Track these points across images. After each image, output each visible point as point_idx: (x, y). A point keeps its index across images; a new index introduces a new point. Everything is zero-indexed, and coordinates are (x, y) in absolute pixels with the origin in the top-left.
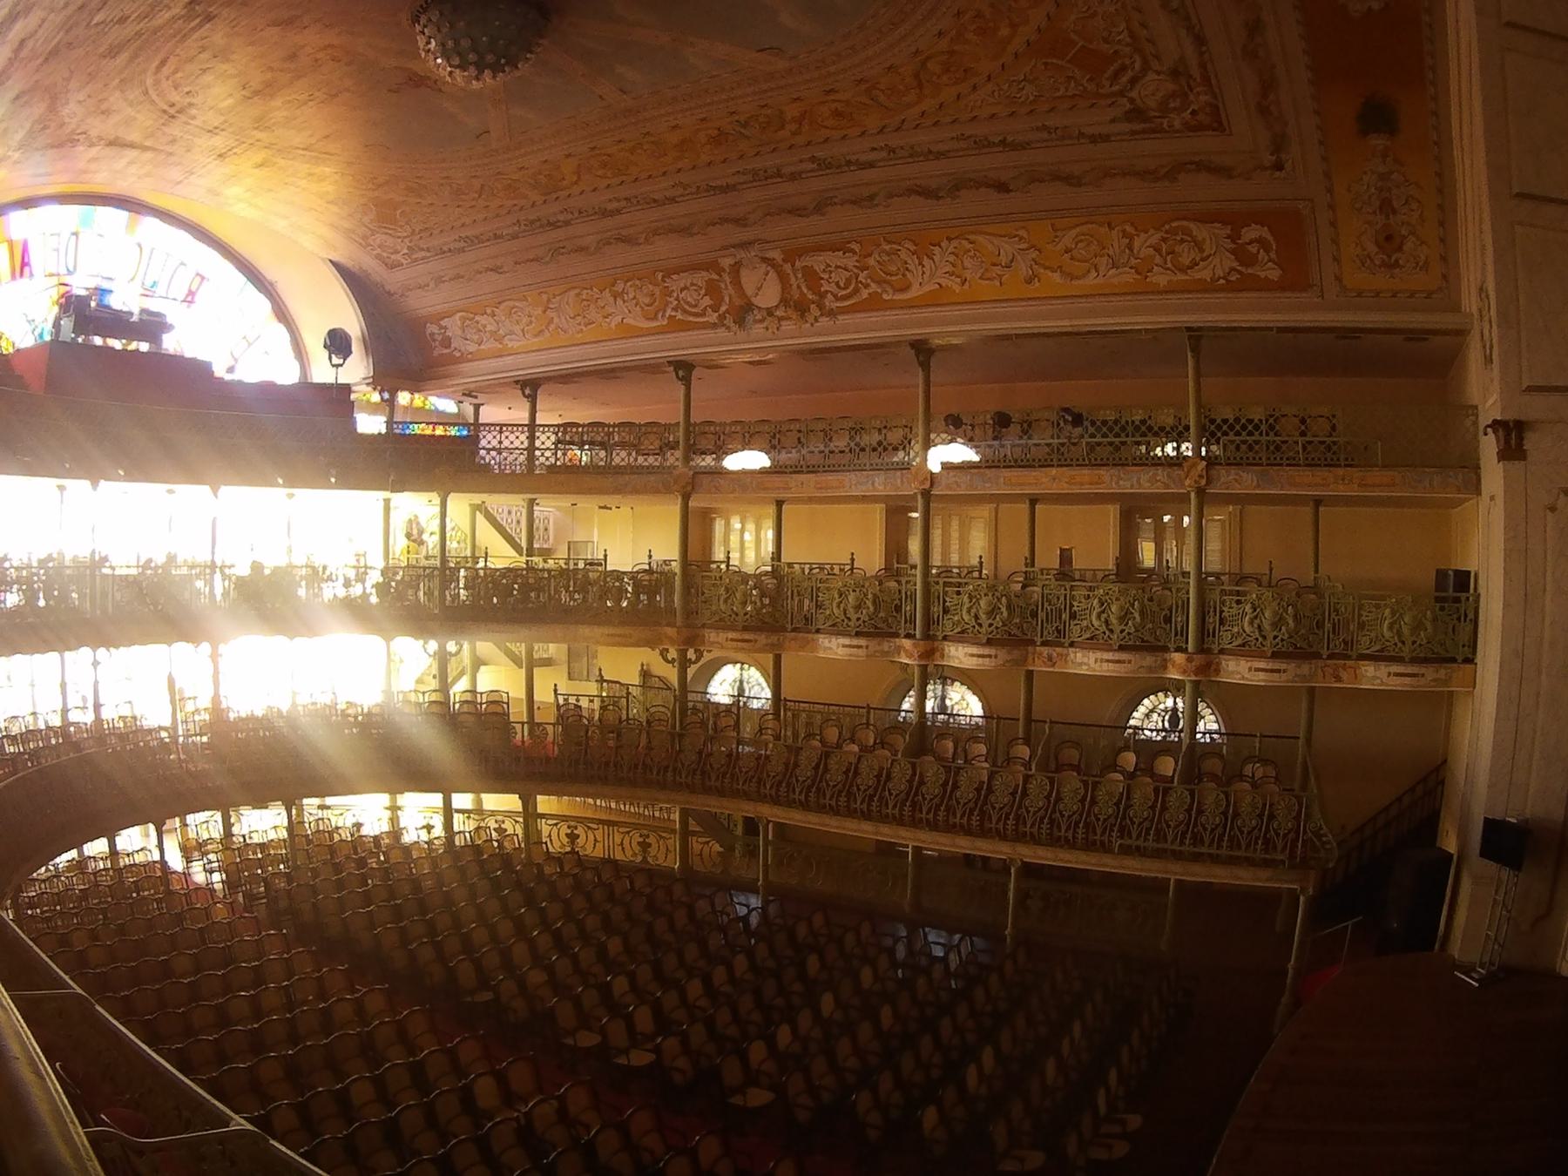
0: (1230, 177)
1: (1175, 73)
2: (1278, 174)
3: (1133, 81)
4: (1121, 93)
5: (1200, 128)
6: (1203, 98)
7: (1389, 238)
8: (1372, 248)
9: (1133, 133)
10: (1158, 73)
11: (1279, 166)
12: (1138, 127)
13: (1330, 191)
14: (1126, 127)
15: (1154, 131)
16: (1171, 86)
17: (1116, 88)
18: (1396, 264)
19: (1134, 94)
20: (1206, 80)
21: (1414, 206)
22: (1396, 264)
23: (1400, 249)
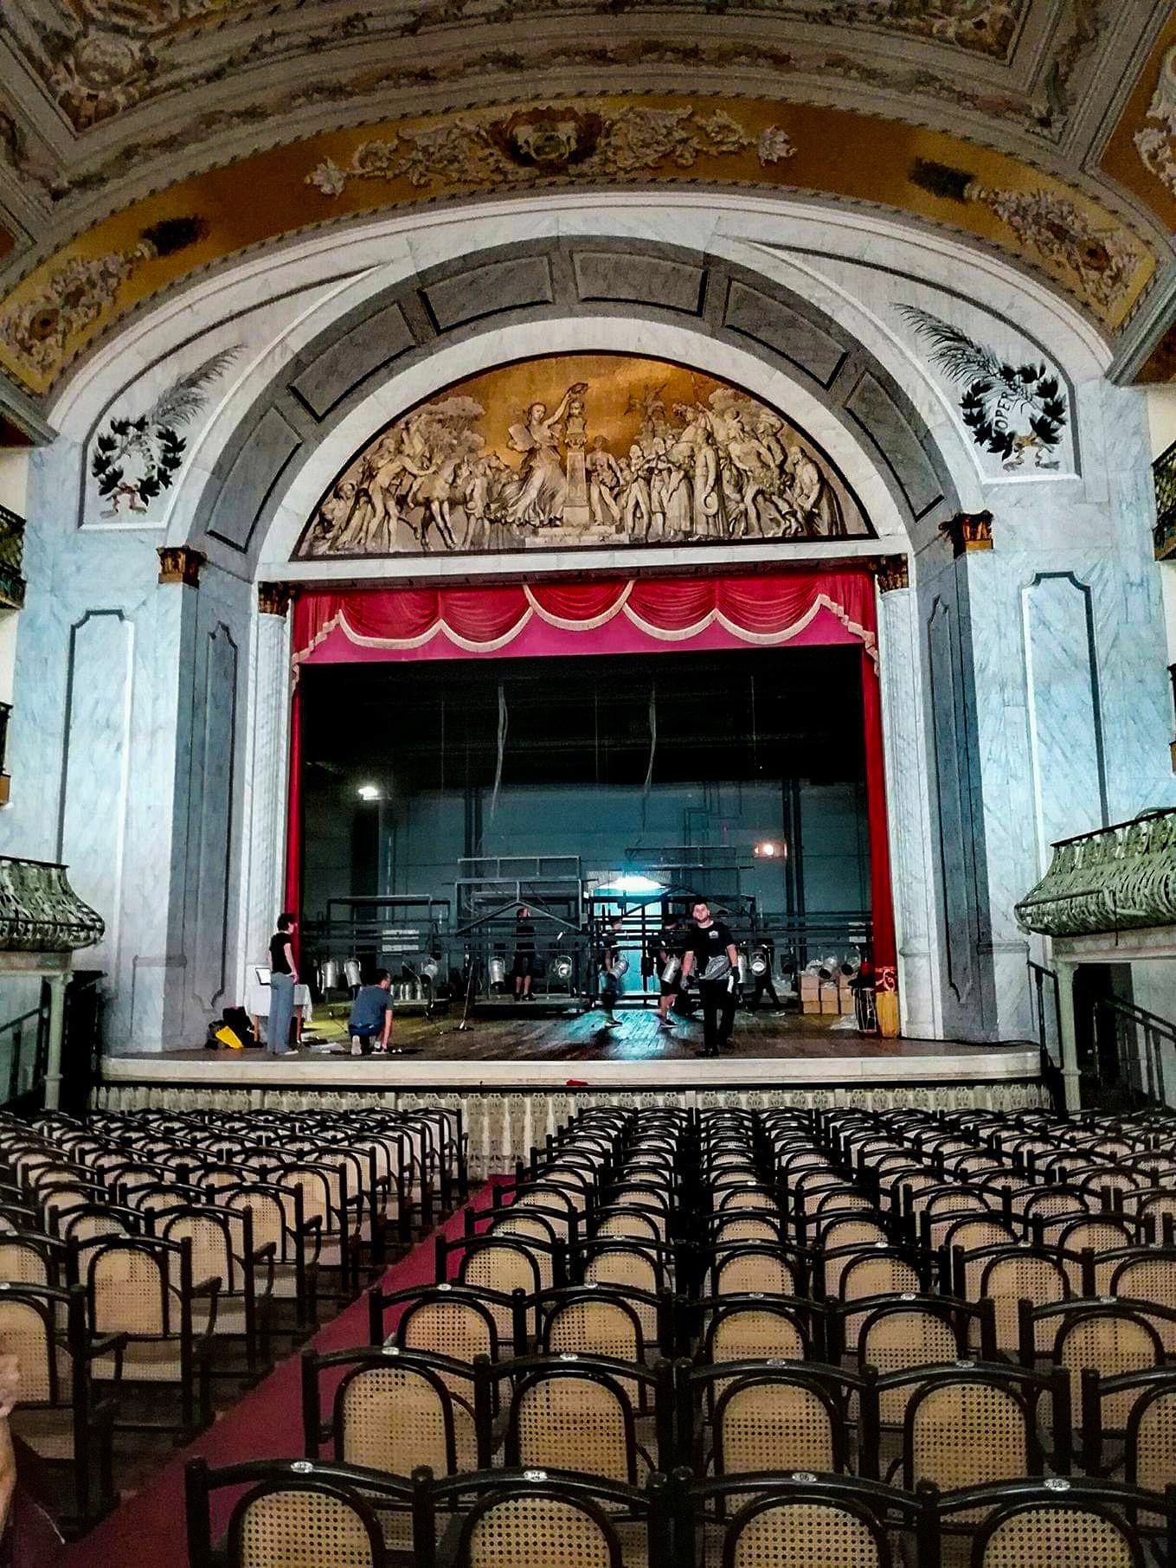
0: (15, 164)
1: (150, 65)
2: (47, 200)
3: (120, 30)
4: (88, 20)
5: (75, 115)
6: (121, 99)
7: (46, 323)
8: (26, 322)
9: (27, 51)
10: (141, 50)
11: (57, 195)
12: (40, 52)
13: (57, 249)
14: (31, 39)
15: (41, 69)
16: (126, 65)
17: (99, 15)
18: (29, 350)
19: (92, 32)
20: (154, 92)
21: (92, 313)
22: (29, 350)
23: (43, 338)
